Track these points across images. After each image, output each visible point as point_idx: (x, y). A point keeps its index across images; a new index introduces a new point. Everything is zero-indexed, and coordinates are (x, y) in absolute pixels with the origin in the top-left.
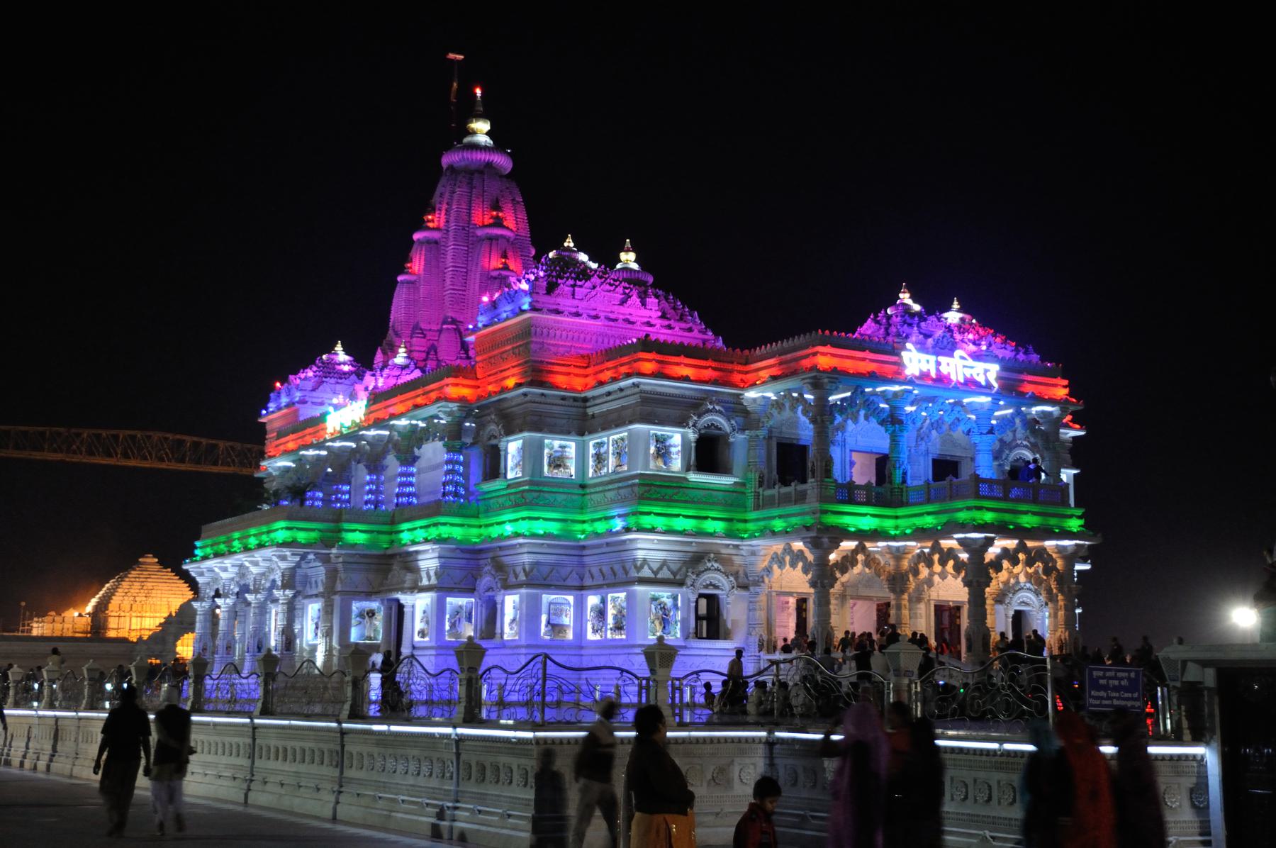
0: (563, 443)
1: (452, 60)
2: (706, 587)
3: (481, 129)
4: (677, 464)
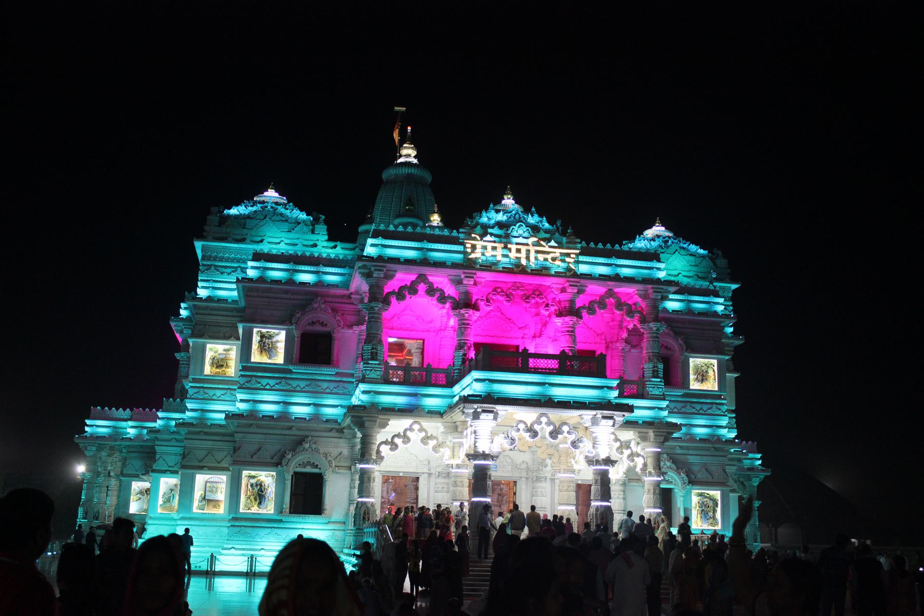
0: (227, 347)
1: (398, 112)
2: (304, 465)
3: (408, 154)
4: (280, 359)
